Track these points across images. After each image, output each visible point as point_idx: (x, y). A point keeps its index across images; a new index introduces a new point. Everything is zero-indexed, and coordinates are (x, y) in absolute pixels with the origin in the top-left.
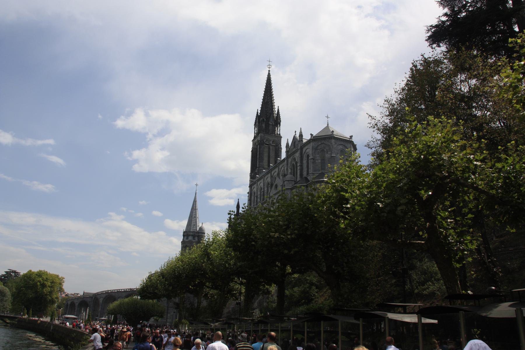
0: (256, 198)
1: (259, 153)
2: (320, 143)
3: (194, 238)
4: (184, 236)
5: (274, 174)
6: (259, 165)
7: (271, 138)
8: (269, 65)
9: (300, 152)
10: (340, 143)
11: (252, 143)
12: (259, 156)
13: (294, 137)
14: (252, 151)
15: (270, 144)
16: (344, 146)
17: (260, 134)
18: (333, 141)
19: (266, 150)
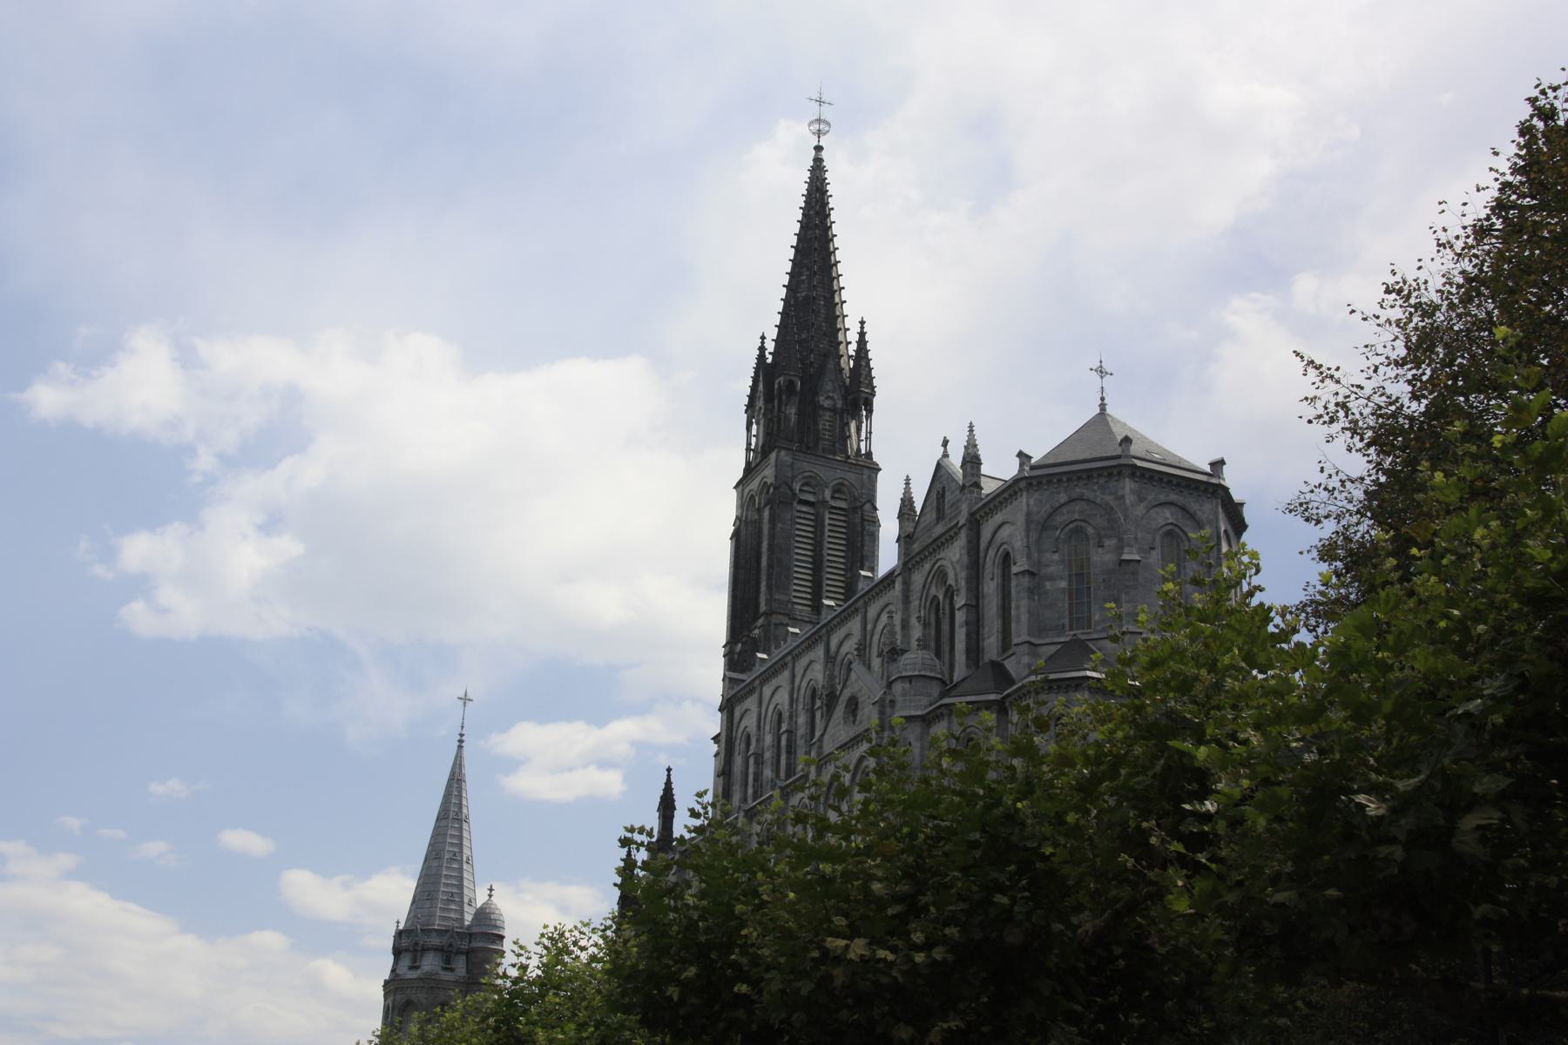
0: (757, 763)
1: (771, 546)
2: (1063, 498)
3: (448, 961)
4: (397, 952)
5: (841, 644)
6: (768, 602)
7: (829, 475)
8: (819, 121)
9: (969, 542)
10: (1162, 498)
11: (734, 494)
12: (770, 558)
13: (939, 466)
14: (736, 536)
15: (824, 502)
16: (1183, 509)
17: (773, 455)
18: (1128, 485)
19: (804, 528)
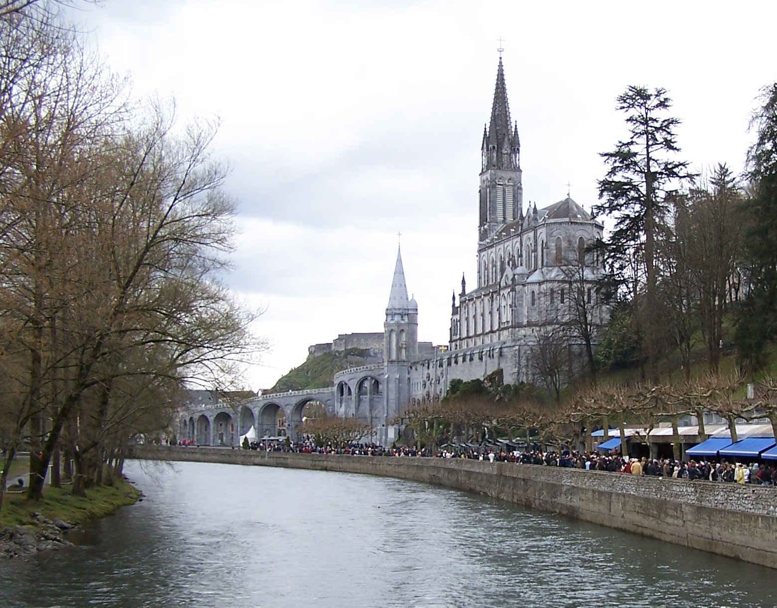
1: (490, 201)
3: (402, 317)
4: (387, 315)
6: (490, 218)
11: (479, 178)
17: (489, 171)
19: (500, 193)
